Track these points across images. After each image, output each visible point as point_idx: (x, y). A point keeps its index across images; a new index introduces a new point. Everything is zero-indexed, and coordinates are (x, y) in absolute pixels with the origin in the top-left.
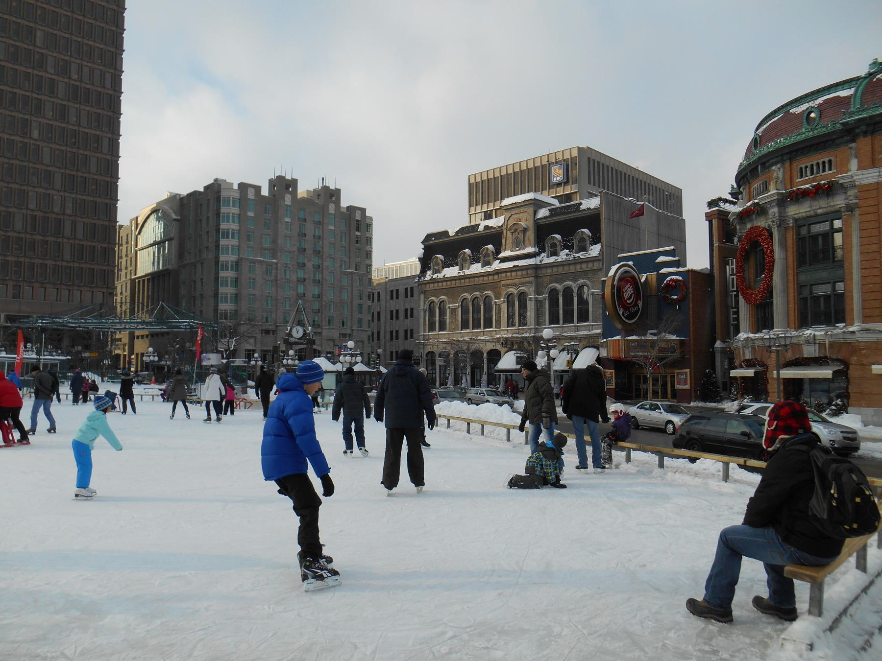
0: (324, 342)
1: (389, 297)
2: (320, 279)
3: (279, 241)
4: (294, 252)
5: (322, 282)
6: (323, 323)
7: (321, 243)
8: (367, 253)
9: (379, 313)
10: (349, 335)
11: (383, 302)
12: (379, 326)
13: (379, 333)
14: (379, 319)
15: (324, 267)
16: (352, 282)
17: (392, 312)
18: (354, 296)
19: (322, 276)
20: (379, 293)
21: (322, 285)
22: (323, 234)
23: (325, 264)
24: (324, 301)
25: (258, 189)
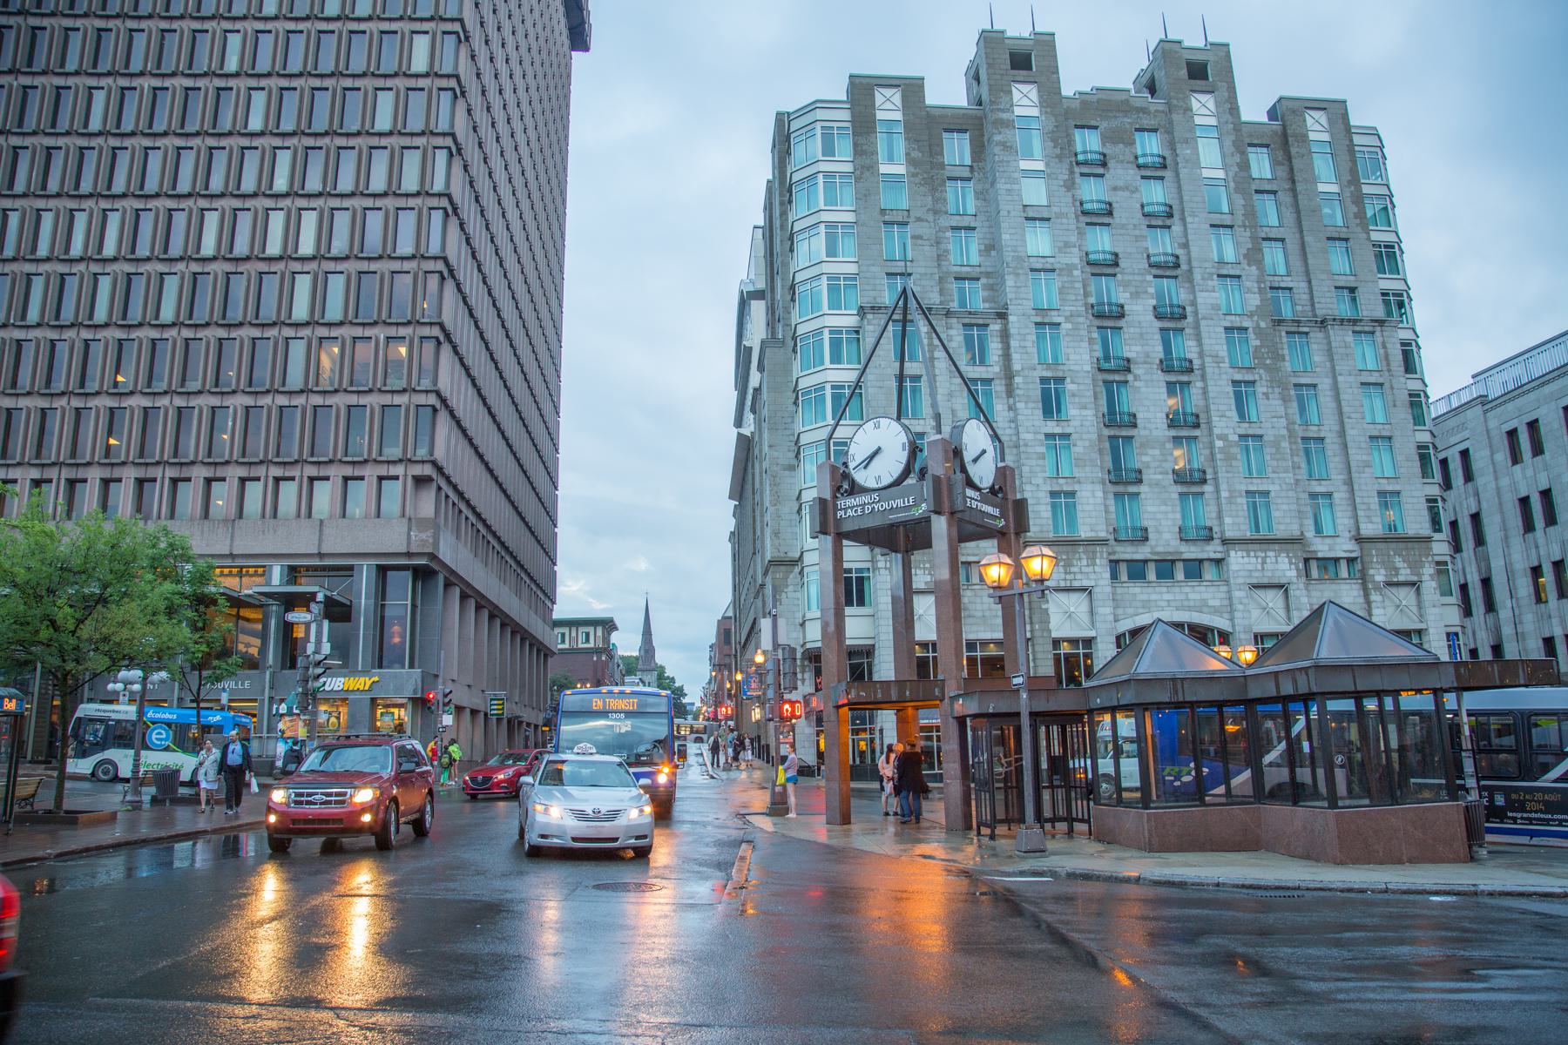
0: (1237, 594)
1: (1503, 456)
2: (1193, 356)
3: (1004, 237)
4: (1070, 268)
5: (1203, 368)
6: (1227, 520)
7: (1177, 228)
8: (1379, 256)
9: (1476, 518)
10: (1350, 561)
11: (1484, 479)
12: (1484, 561)
13: (1486, 583)
14: (1480, 540)
15: (1202, 311)
16: (1332, 360)
17: (1524, 502)
18: (1345, 409)
19: (1200, 344)
20: (1465, 454)
21: (1203, 378)
22: (1181, 198)
23: (1203, 299)
24: (1223, 437)
25: (912, 89)
